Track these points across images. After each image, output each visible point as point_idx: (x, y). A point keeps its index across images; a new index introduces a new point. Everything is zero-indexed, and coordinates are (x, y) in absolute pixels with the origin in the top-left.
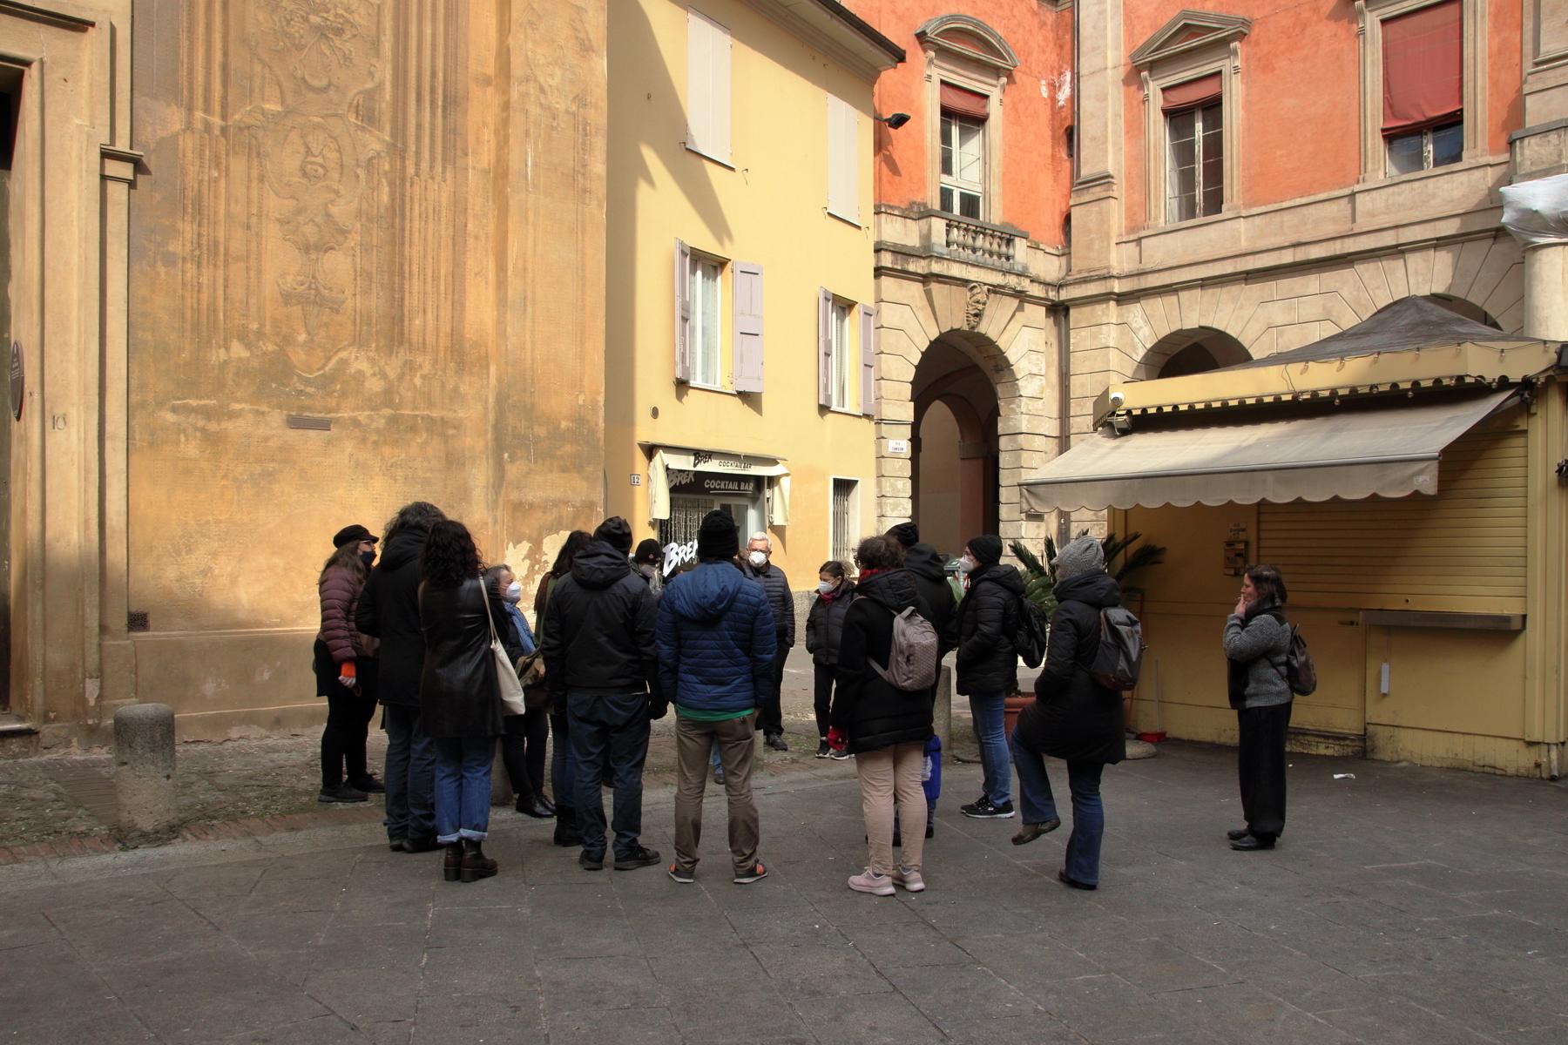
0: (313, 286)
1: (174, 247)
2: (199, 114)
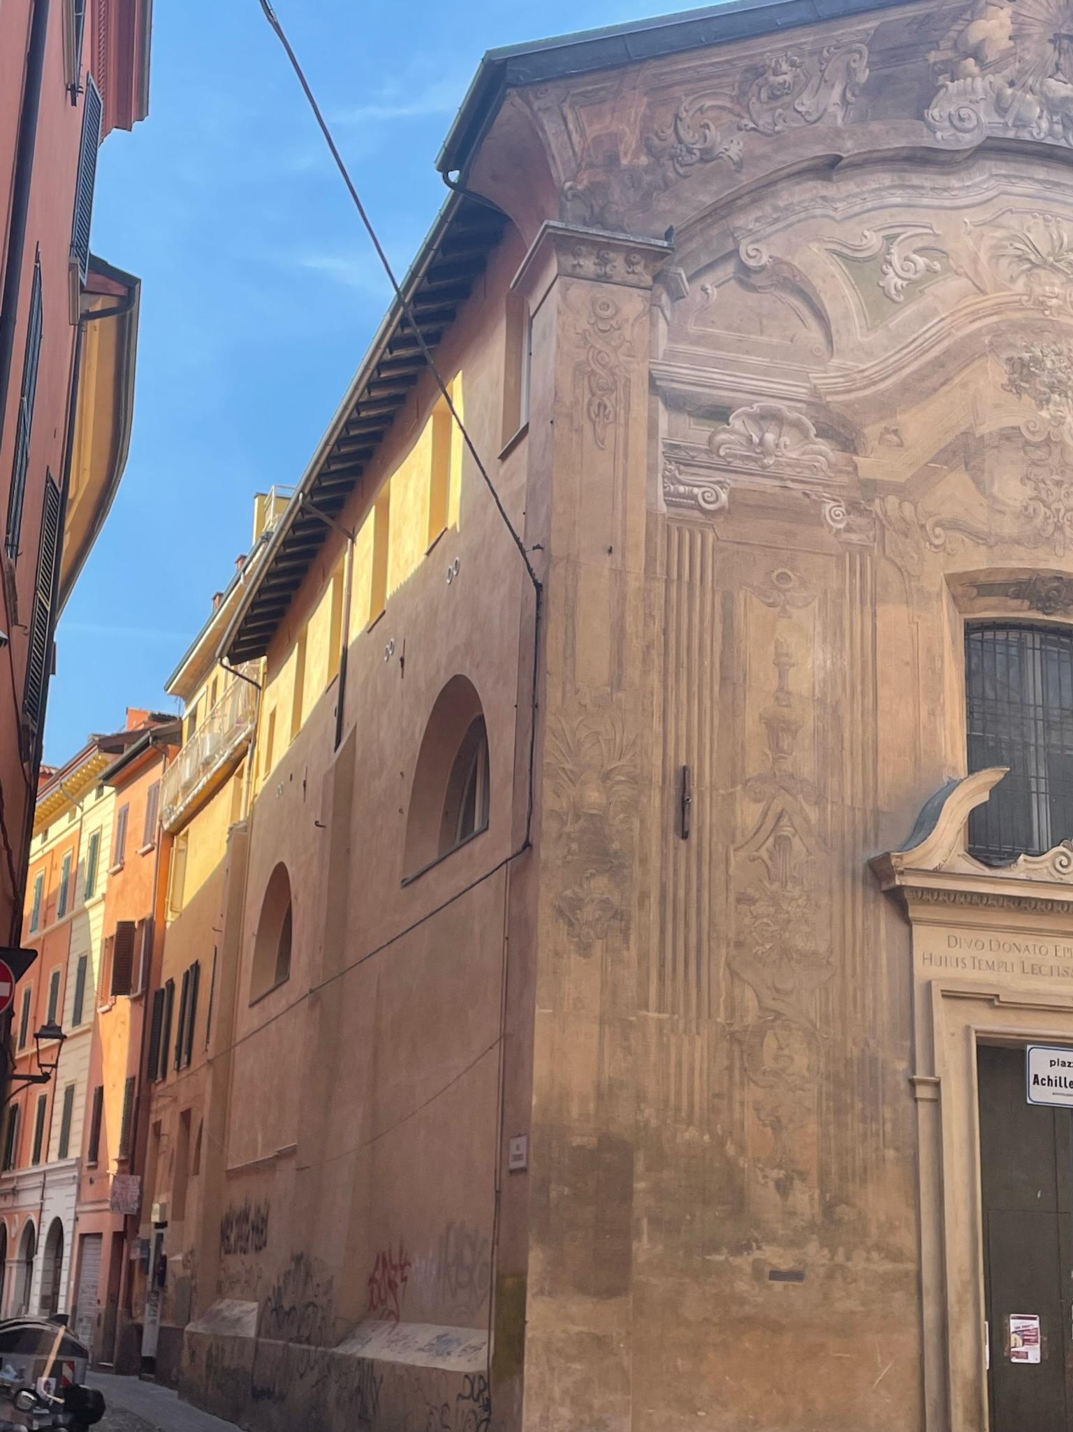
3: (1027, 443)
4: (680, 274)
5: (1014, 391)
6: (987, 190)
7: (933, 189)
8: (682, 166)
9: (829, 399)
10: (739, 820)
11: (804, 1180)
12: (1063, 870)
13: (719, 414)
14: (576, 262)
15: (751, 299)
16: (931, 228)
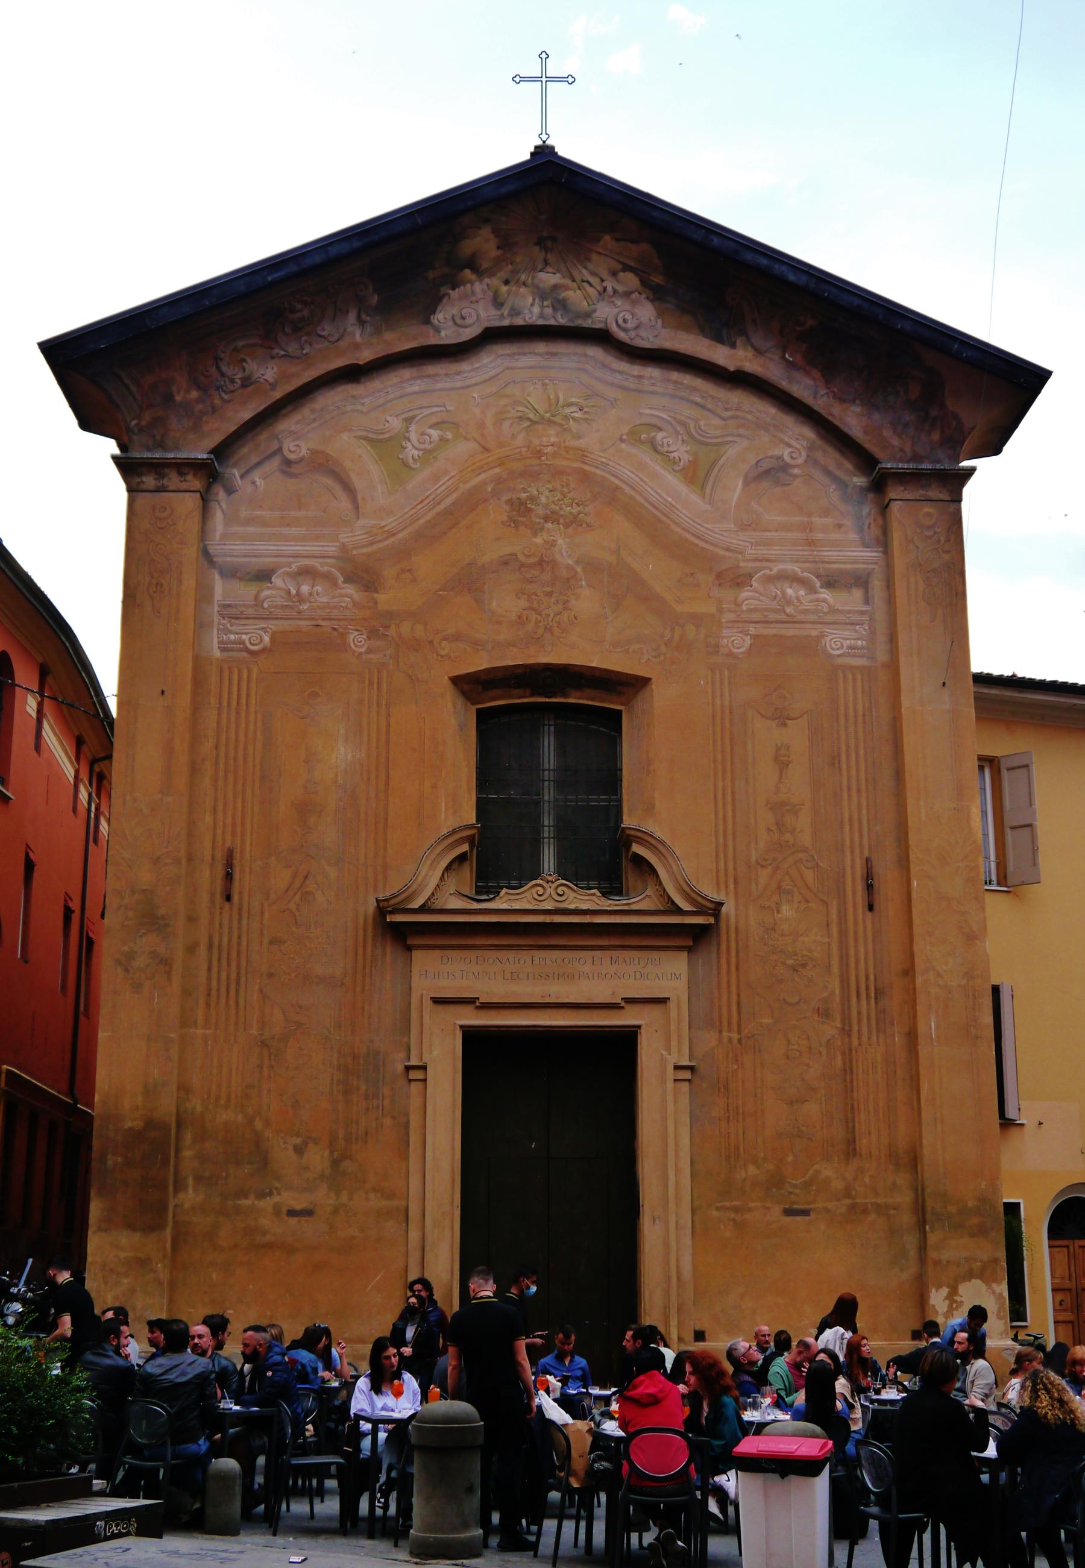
0: (796, 1126)
2: (725, 1034)
3: (522, 565)
4: (234, 475)
5: (512, 525)
6: (494, 368)
8: (226, 393)
9: (355, 552)
11: (316, 1144)
13: (264, 576)
14: (139, 480)
16: (445, 407)
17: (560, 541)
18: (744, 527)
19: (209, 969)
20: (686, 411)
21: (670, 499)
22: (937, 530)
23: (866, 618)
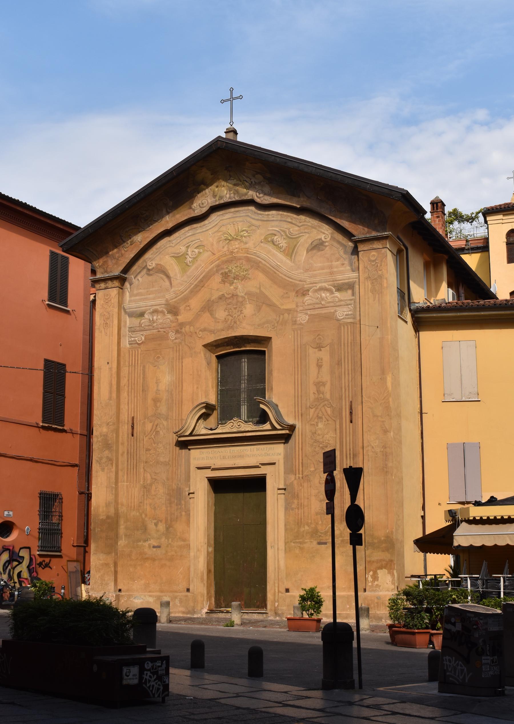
1: (293, 506)
2: (297, 475)
3: (226, 298)
6: (216, 221)
7: (200, 227)
9: (171, 301)
10: (146, 428)
12: (239, 427)
13: (142, 315)
15: (150, 278)
17: (239, 287)
18: (307, 270)
19: (128, 461)
20: (285, 226)
21: (279, 264)
22: (377, 261)
23: (353, 302)
